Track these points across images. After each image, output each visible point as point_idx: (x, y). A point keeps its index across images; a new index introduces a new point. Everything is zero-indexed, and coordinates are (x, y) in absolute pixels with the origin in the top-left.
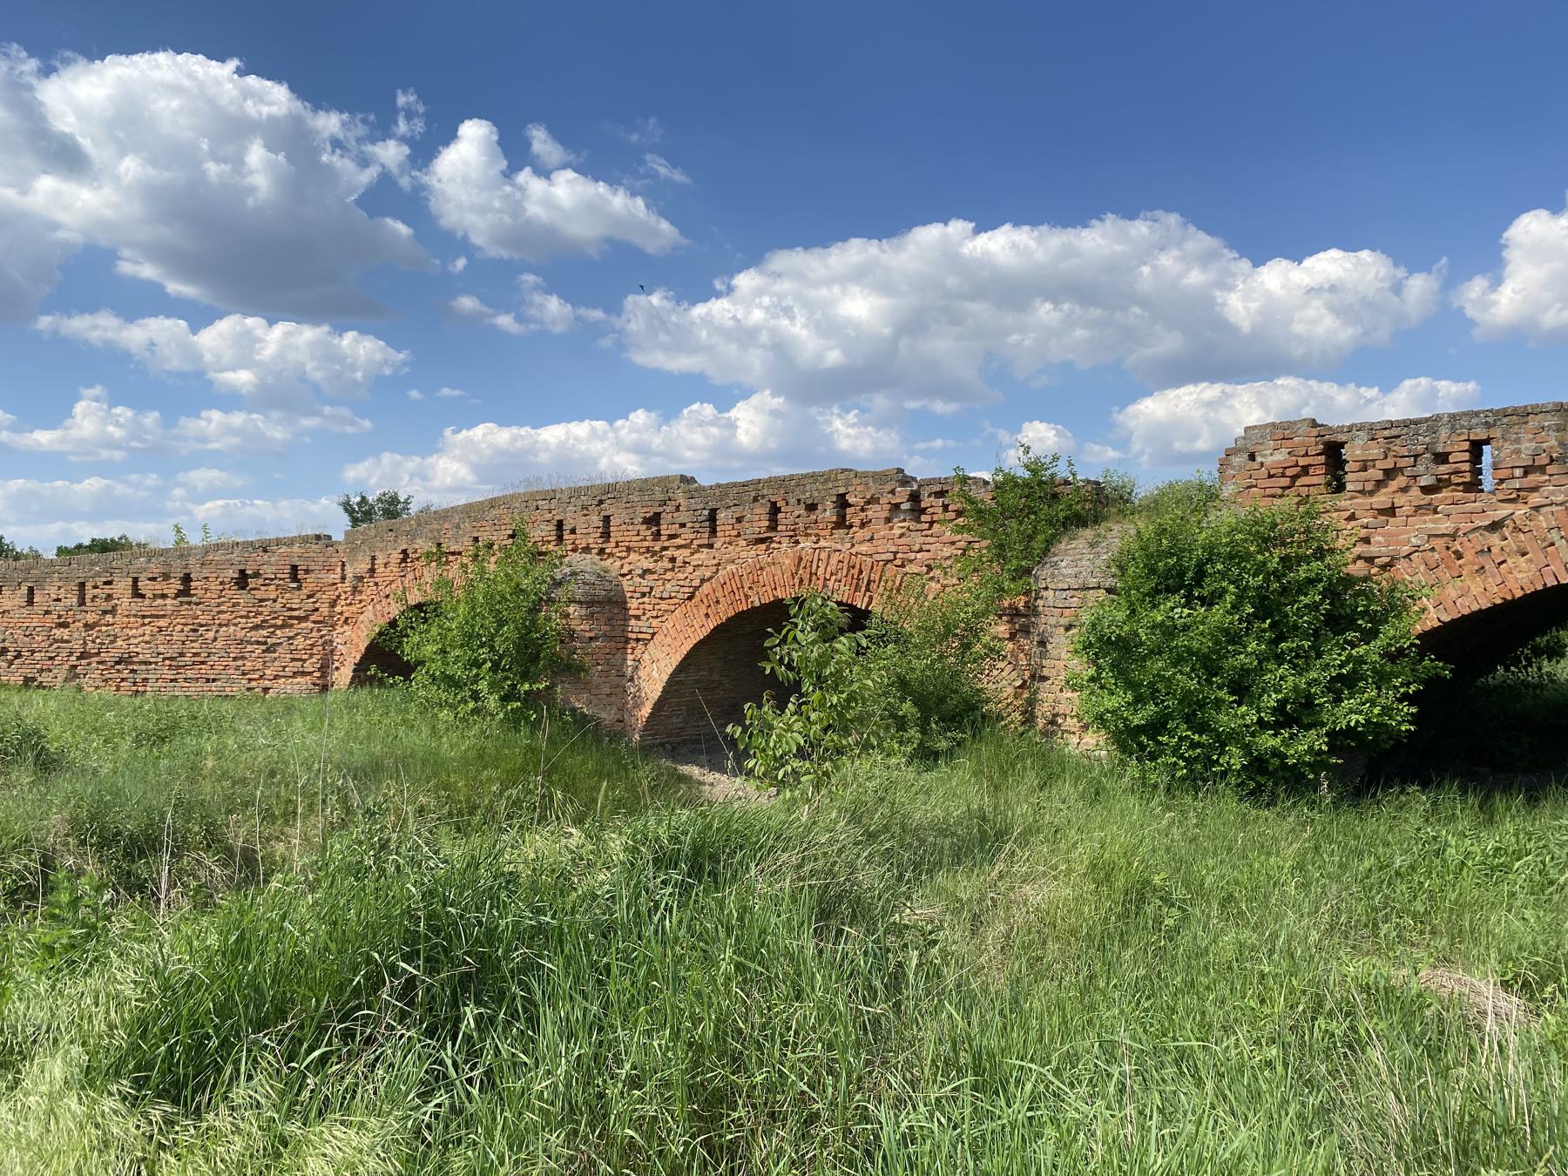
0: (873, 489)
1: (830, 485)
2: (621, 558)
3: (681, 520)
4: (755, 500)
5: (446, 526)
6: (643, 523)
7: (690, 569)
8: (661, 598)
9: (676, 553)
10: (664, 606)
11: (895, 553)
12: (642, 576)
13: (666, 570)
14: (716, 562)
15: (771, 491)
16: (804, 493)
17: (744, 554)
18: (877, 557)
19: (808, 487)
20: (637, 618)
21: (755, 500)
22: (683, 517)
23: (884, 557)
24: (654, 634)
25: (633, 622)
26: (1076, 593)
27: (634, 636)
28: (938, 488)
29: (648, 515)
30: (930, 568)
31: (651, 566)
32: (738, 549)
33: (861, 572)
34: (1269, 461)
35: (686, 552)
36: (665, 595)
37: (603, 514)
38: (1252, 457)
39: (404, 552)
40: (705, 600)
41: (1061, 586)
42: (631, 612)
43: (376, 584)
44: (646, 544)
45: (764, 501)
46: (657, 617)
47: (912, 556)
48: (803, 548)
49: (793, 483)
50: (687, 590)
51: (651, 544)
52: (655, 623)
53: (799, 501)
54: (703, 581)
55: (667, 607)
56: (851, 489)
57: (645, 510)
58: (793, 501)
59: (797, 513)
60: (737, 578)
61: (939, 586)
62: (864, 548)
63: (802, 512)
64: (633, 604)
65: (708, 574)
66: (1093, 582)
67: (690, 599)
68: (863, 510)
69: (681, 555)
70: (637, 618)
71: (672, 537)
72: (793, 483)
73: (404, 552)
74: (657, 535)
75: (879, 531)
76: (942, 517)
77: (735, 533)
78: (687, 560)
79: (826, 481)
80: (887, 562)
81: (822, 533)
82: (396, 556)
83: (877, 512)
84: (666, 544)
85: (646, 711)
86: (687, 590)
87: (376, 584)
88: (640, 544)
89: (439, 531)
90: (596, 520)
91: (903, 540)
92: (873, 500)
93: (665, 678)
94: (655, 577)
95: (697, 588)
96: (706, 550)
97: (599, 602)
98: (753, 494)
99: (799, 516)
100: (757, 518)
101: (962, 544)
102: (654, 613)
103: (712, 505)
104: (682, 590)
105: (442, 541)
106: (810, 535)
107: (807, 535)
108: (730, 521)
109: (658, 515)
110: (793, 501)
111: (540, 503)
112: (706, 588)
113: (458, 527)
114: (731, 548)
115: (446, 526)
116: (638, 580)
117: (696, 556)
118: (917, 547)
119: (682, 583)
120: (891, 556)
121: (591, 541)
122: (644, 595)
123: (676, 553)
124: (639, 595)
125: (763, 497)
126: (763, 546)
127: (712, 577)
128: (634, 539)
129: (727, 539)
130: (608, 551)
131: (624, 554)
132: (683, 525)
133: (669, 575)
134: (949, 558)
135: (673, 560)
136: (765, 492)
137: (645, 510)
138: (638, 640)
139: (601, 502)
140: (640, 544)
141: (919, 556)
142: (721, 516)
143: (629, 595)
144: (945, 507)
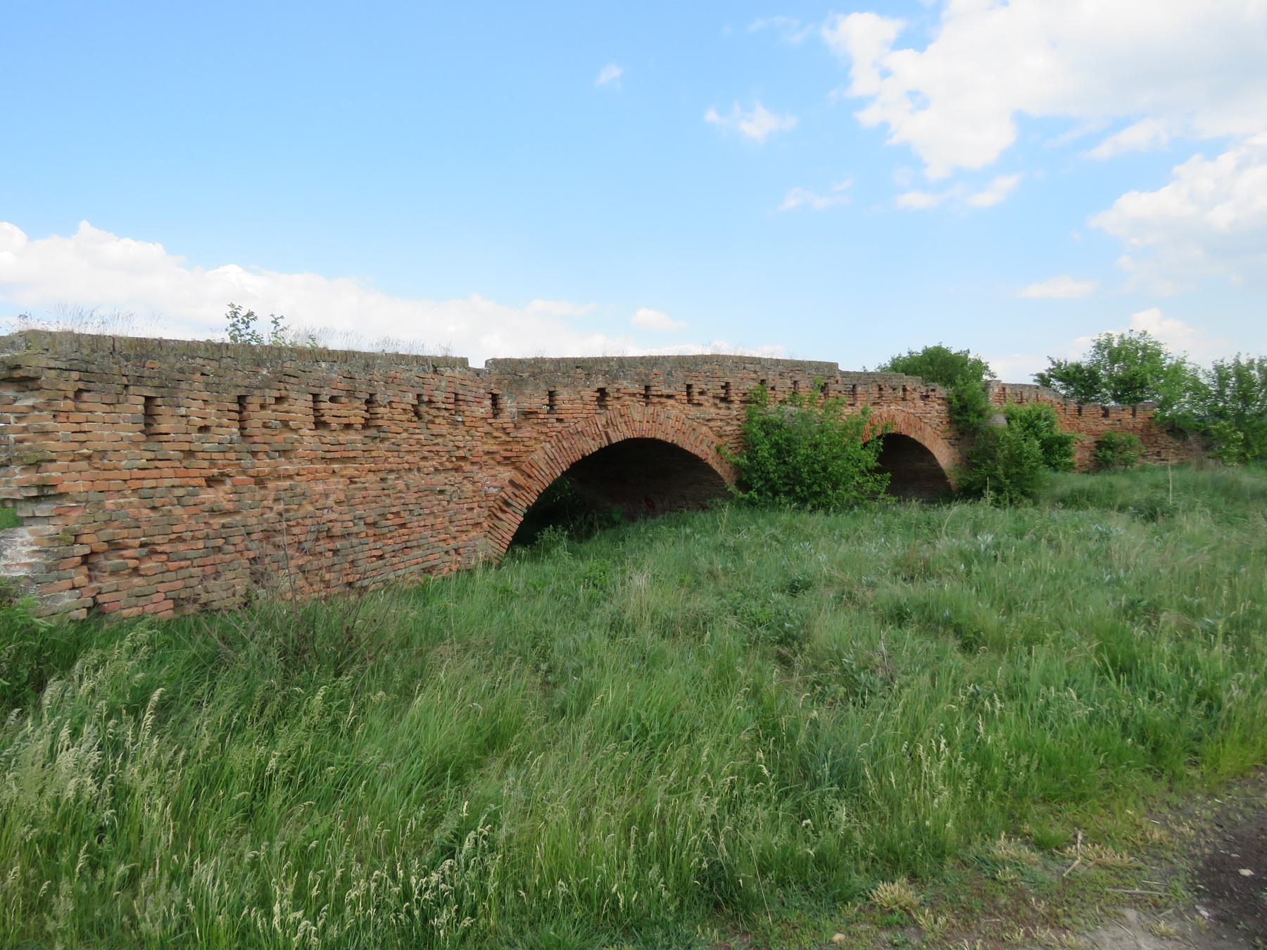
5: (655, 370)
22: (839, 387)
39: (602, 392)
43: (559, 420)
73: (602, 392)
82: (589, 394)
83: (916, 395)
89: (647, 375)
90: (789, 383)
92: (915, 390)
103: (854, 382)
105: (652, 384)
111: (747, 365)
113: (670, 374)
115: (655, 370)
142: (859, 389)
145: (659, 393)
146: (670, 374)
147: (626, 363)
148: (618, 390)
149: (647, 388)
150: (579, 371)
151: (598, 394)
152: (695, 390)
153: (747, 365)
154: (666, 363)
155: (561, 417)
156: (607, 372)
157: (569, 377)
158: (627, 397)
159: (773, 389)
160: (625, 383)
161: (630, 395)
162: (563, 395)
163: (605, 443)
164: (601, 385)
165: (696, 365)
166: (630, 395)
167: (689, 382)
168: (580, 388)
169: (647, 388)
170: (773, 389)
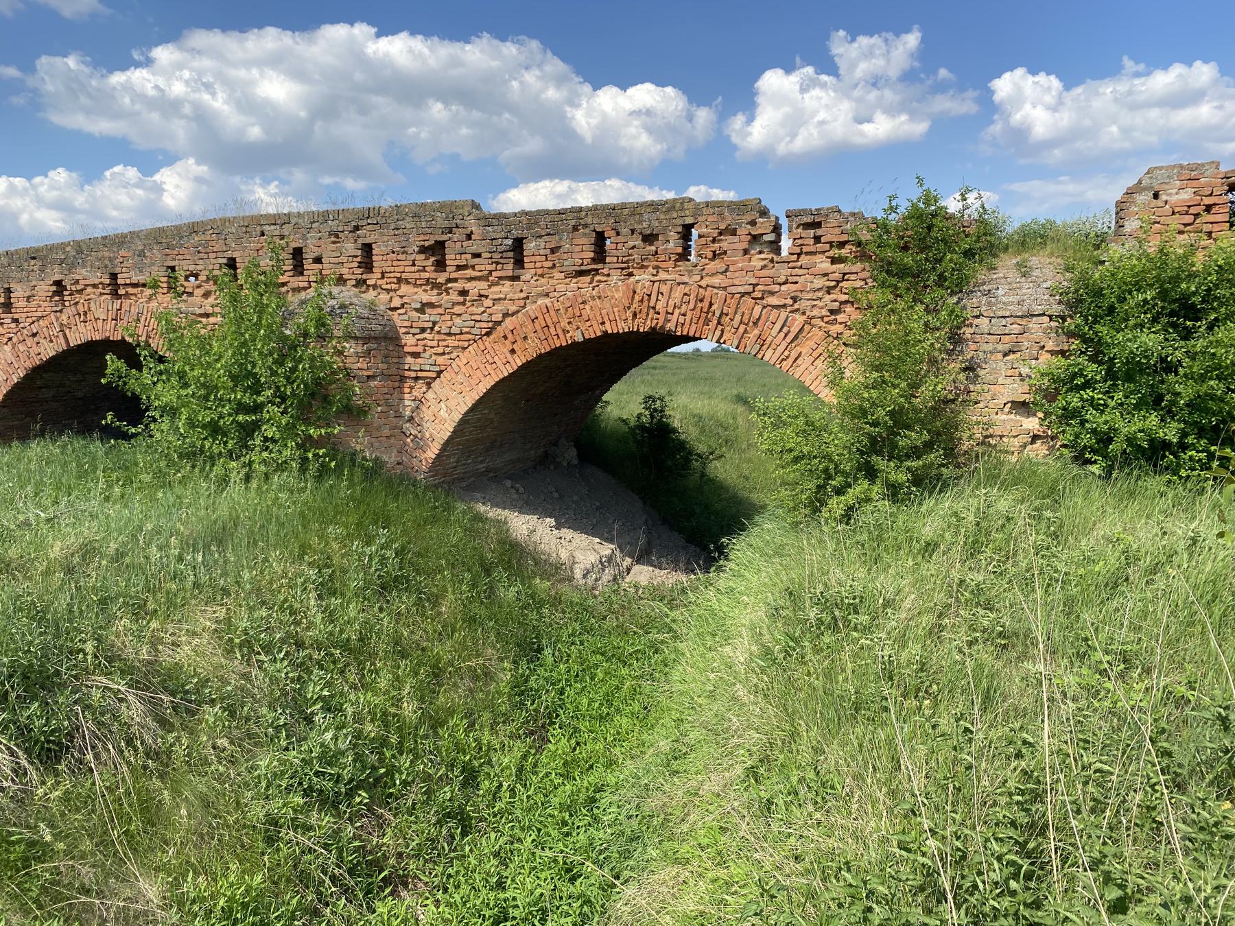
0: (729, 219)
1: (675, 215)
2: (388, 291)
3: (475, 249)
4: (575, 229)
5: (123, 253)
6: (420, 252)
7: (488, 303)
8: (449, 334)
9: (468, 286)
10: (451, 342)
11: (755, 286)
12: (421, 310)
13: (454, 304)
14: (523, 295)
15: (596, 220)
16: (640, 222)
17: (561, 287)
18: (733, 289)
19: (646, 217)
20: (416, 355)
21: (575, 229)
23: (741, 289)
24: (439, 373)
25: (409, 359)
26: (1018, 320)
27: (413, 374)
28: (809, 219)
29: (427, 244)
30: (795, 299)
31: (433, 300)
32: (555, 282)
33: (711, 304)
34: (1174, 199)
35: (484, 285)
36: (454, 330)
37: (360, 241)
38: (1156, 196)
39: (58, 283)
40: (510, 336)
41: (1001, 313)
42: (406, 349)
43: (16, 321)
44: (426, 275)
45: (587, 231)
46: (444, 354)
47: (777, 288)
48: (637, 282)
49: (626, 212)
50: (484, 325)
51: (433, 275)
52: (440, 360)
53: (633, 231)
54: (506, 315)
55: (456, 343)
56: (700, 219)
57: (422, 238)
58: (625, 231)
59: (631, 244)
60: (552, 312)
61: (804, 318)
62: (716, 281)
63: (639, 243)
64: (409, 341)
65: (513, 308)
66: (1038, 309)
67: (488, 334)
68: (714, 241)
69: (475, 288)
70: (416, 355)
71: (459, 268)
72: (626, 212)
74: (441, 265)
75: (735, 263)
76: (812, 249)
77: (550, 264)
78: (483, 292)
79: (669, 210)
80: (743, 294)
81: (663, 265)
82: (44, 289)
84: (454, 275)
85: (432, 452)
86: (484, 325)
87: (16, 321)
88: (417, 275)
89: (111, 259)
90: (351, 248)
91: (765, 272)
93: (457, 417)
94: (441, 311)
95: (499, 323)
96: (508, 283)
97: (376, 338)
98: (573, 222)
99: (633, 247)
100: (578, 248)
101: (837, 276)
102: (440, 350)
103: (515, 234)
104: (477, 325)
105: (117, 270)
106: (647, 267)
107: (643, 267)
108: (542, 252)
109: (441, 245)
110: (625, 231)
111: (266, 228)
112: (509, 323)
113: (142, 254)
114: (543, 281)
115: (123, 253)
116: (415, 314)
117: (494, 289)
118: (782, 279)
119: (478, 318)
120: (750, 289)
121: (344, 271)
122: (423, 330)
123: (468, 286)
124: (418, 331)
125: (586, 226)
126: (588, 279)
127: (517, 312)
128: (407, 269)
129: (539, 271)
130: (369, 282)
131: (394, 286)
132: (478, 255)
133: (457, 309)
134: (819, 290)
135: (464, 293)
136: (589, 220)
137: (422, 238)
138: (417, 379)
139: (357, 228)
140: (417, 275)
141: (784, 288)
142: (530, 246)
143: (403, 330)
144: (817, 239)
145: (128, 281)
146: (142, 254)
147: (84, 247)
148: (77, 282)
149: (114, 276)
150: (33, 262)
151: (54, 288)
152: (181, 274)
153: (266, 228)
154: (137, 241)
155: (16, 316)
156: (62, 261)
157: (22, 270)
158: (89, 290)
159: (318, 260)
160: (83, 271)
161: (95, 286)
162: (19, 292)
163: (60, 345)
164: (57, 277)
165: (181, 238)
166: (95, 286)
167: (171, 264)
168: (34, 283)
169: (114, 276)
170: (318, 260)
